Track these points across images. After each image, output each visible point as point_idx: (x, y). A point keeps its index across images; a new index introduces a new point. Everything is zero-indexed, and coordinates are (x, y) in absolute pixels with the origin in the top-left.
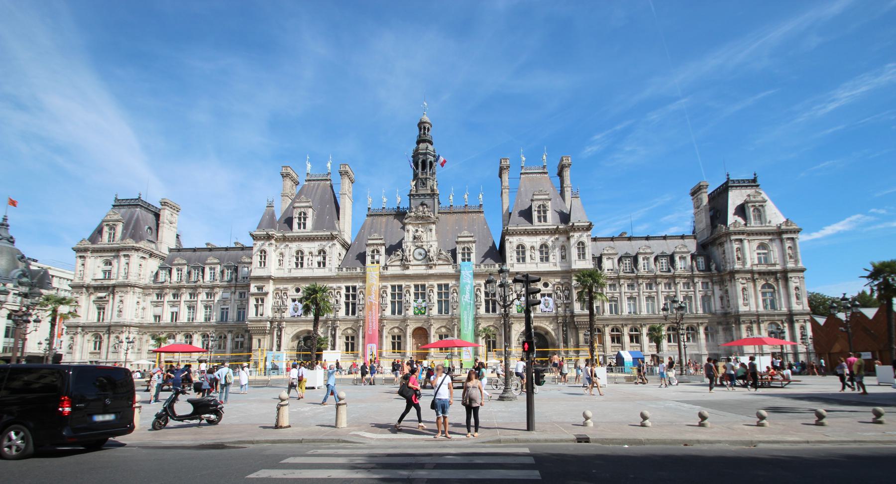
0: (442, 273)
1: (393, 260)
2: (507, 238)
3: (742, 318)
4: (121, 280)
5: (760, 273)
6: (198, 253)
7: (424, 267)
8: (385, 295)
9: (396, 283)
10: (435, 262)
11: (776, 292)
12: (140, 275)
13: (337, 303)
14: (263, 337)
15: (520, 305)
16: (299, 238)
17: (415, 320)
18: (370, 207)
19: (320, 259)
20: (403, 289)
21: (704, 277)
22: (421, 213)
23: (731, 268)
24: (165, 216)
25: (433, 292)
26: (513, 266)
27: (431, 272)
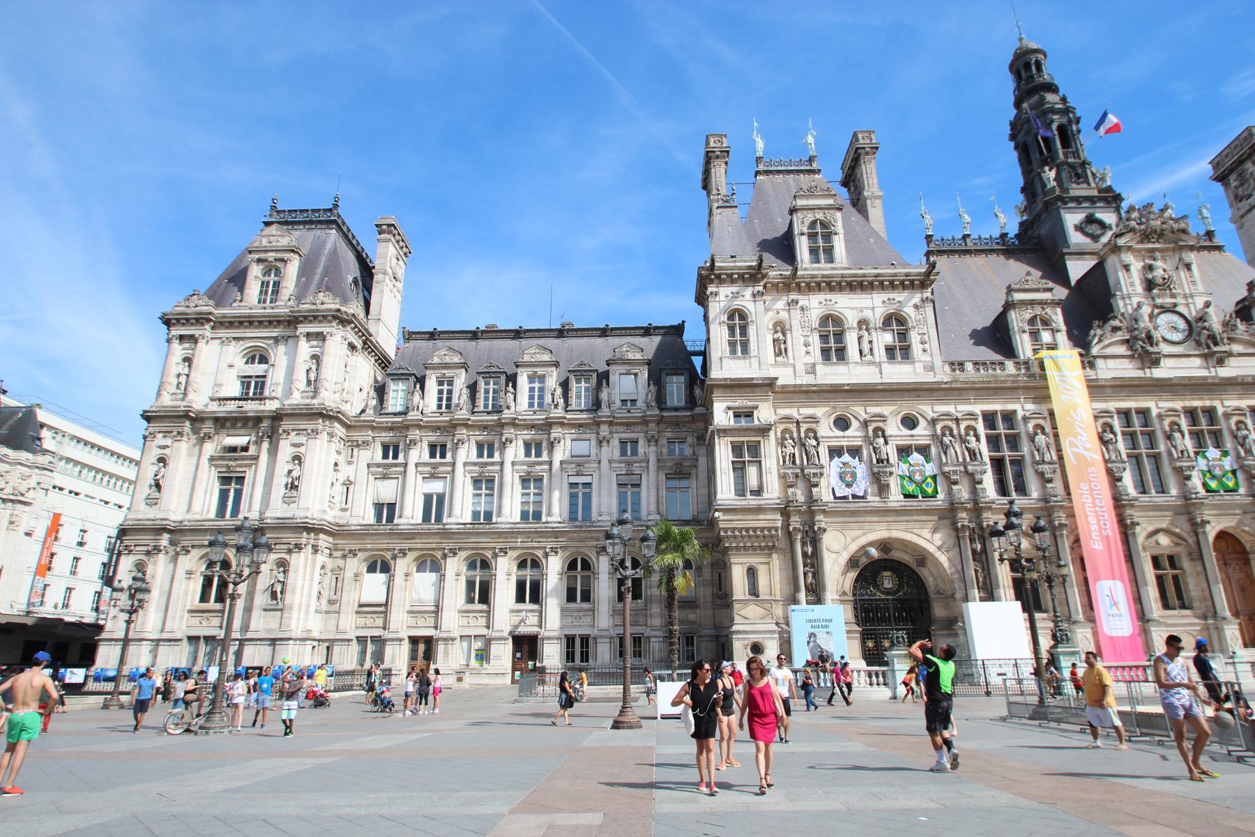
1: (1107, 342)
4: (297, 399)
6: (484, 344)
7: (1197, 362)
10: (1226, 348)
13: (971, 459)
14: (765, 560)
16: (828, 284)
17: (1214, 507)
18: (931, 233)
19: (888, 338)
20: (1156, 422)
27: (1224, 372)
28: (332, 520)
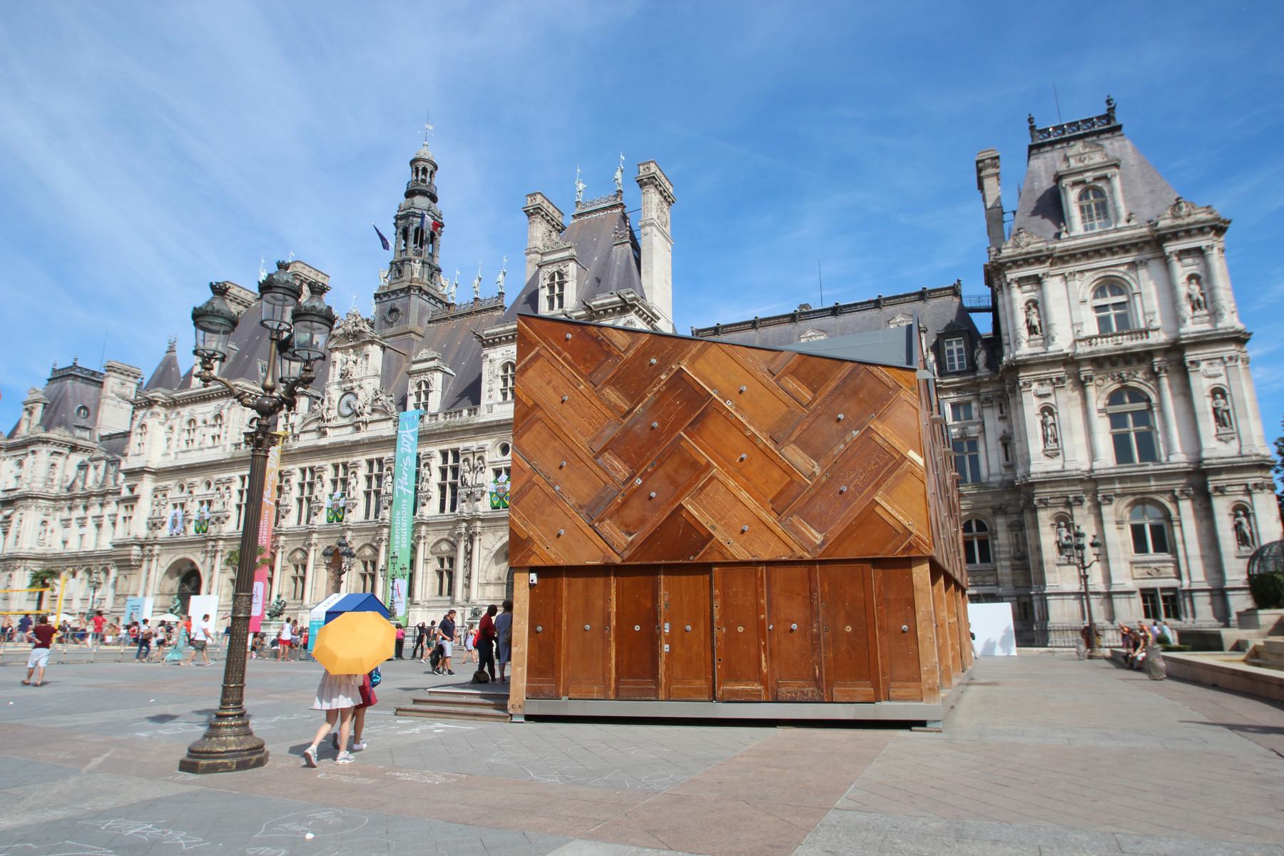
0: (374, 438)
2: (485, 352)
3: (1041, 493)
5: (1099, 362)
7: (350, 429)
8: (287, 488)
9: (306, 465)
10: (366, 417)
11: (1155, 409)
12: (52, 480)
15: (496, 493)
17: (327, 532)
19: (216, 431)
21: (957, 390)
22: (350, 327)
23: (1012, 356)
24: (109, 387)
25: (355, 476)
26: (490, 411)
27: (357, 437)
28: (41, 552)
